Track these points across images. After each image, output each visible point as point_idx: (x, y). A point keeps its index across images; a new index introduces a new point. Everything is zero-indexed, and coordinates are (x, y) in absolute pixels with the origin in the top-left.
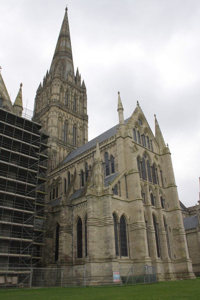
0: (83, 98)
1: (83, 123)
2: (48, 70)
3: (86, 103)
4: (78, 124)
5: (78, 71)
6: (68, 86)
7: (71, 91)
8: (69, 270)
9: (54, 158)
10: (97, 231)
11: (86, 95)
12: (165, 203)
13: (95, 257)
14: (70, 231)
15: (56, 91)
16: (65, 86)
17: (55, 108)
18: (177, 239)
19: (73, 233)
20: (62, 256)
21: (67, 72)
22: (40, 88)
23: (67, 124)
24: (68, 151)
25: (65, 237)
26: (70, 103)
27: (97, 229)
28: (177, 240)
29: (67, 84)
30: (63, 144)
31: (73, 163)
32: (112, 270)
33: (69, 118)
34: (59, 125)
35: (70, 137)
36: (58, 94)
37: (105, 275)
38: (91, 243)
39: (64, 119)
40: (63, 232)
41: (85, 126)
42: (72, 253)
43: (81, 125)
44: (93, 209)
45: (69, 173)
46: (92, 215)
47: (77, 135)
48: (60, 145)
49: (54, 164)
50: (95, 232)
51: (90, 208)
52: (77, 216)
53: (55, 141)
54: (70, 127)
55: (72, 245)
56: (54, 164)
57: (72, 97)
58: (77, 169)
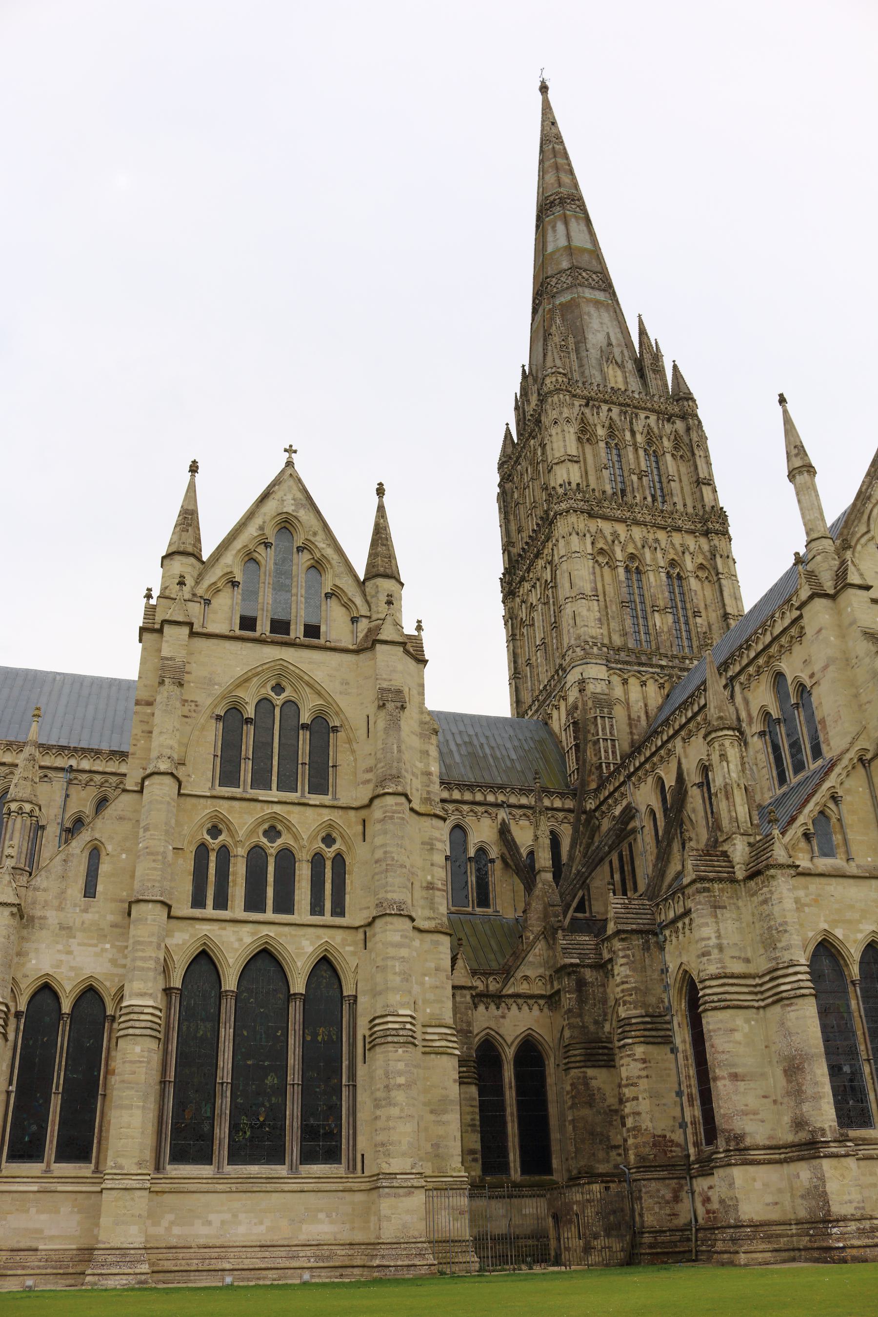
0: (686, 439)
1: (706, 547)
2: (523, 366)
3: (703, 459)
4: (688, 557)
5: (642, 332)
6: (610, 410)
7: (627, 426)
8: (676, 1199)
9: (604, 729)
10: (746, 1028)
11: (700, 422)
13: (748, 1141)
14: (662, 1033)
15: (562, 450)
16: (598, 414)
17: (572, 518)
19: (678, 1041)
20: (639, 1140)
21: (594, 353)
22: (509, 450)
24: (662, 686)
25: (644, 1061)
26: (634, 478)
27: (747, 1021)
29: (605, 402)
30: (632, 659)
31: (668, 741)
32: (825, 1193)
33: (639, 545)
34: (603, 586)
36: (573, 460)
37: (803, 1214)
38: (727, 1082)
39: (619, 555)
40: (630, 1041)
41: (719, 561)
42: (683, 1125)
43: (700, 560)
44: (719, 937)
45: (660, 782)
46: (719, 965)
47: (688, 606)
48: (620, 670)
49: (606, 751)
50: (738, 1036)
51: (705, 935)
52: (681, 971)
53: (597, 656)
55: (679, 1094)
56: (606, 751)
58: (683, 761)
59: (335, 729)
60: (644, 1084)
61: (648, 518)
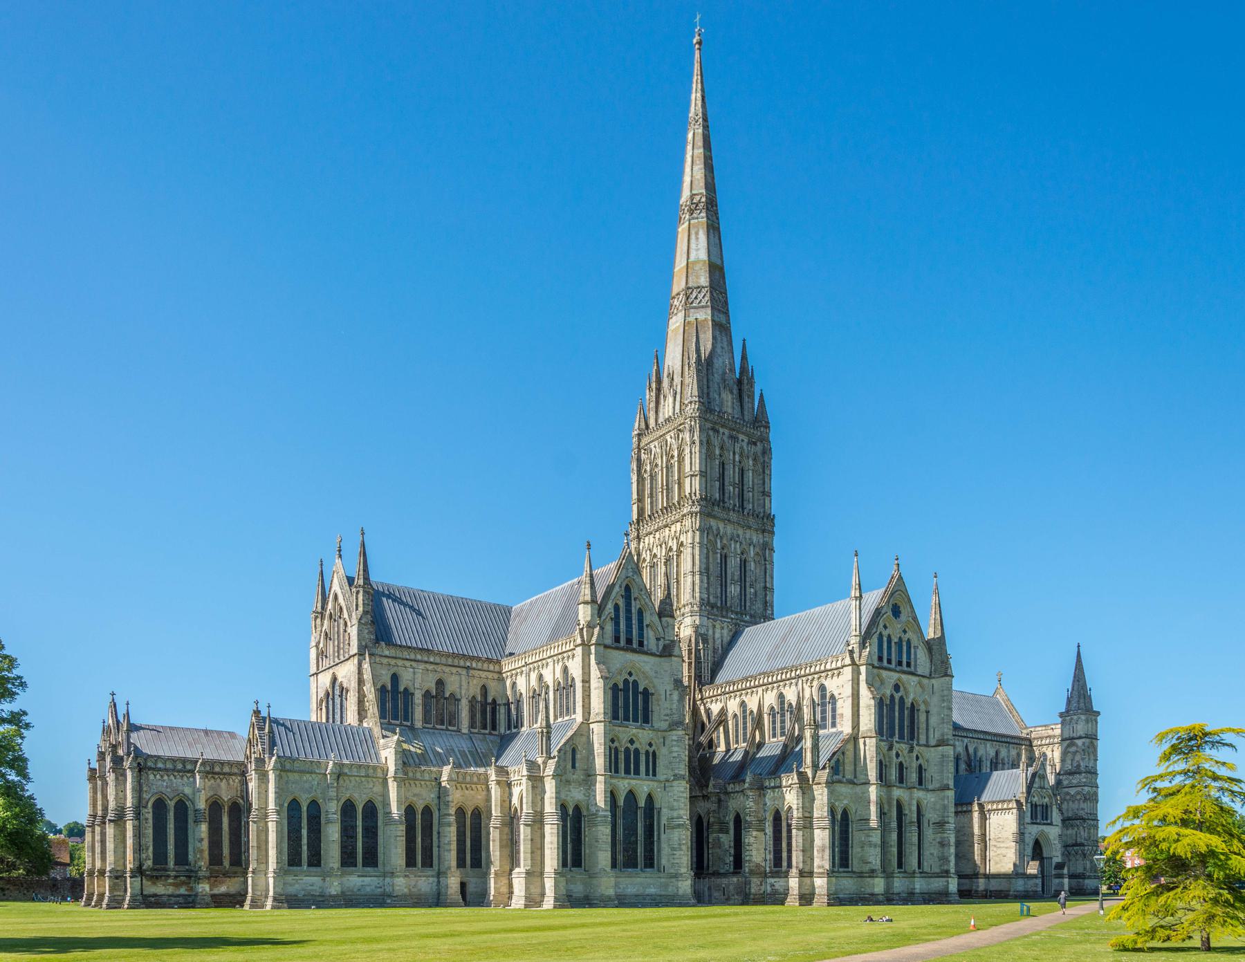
1: (761, 541)
4: (752, 548)
5: (744, 357)
8: (761, 885)
12: (927, 775)
18: (938, 840)
19: (767, 831)
20: (751, 865)
23: (725, 558)
26: (731, 488)
28: (939, 843)
35: (734, 590)
42: (766, 860)
47: (748, 579)
54: (733, 563)
55: (765, 849)
57: (734, 466)
59: (652, 694)
60: (755, 845)
61: (735, 520)
